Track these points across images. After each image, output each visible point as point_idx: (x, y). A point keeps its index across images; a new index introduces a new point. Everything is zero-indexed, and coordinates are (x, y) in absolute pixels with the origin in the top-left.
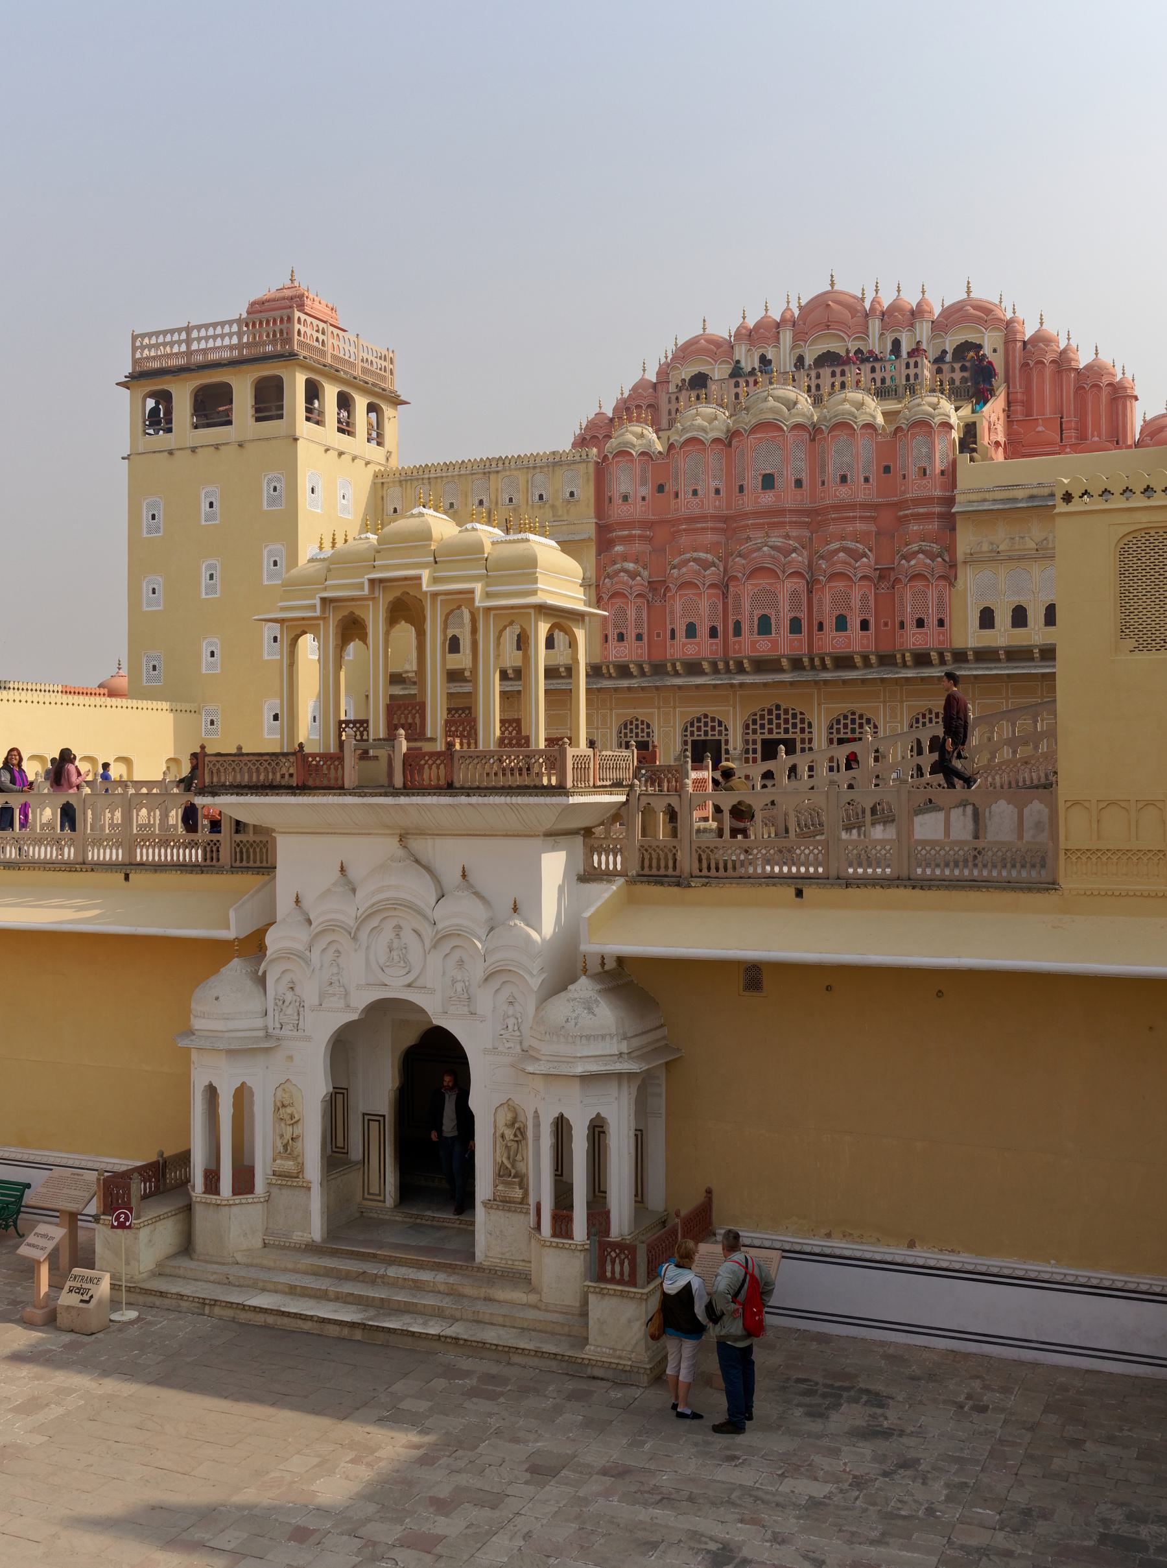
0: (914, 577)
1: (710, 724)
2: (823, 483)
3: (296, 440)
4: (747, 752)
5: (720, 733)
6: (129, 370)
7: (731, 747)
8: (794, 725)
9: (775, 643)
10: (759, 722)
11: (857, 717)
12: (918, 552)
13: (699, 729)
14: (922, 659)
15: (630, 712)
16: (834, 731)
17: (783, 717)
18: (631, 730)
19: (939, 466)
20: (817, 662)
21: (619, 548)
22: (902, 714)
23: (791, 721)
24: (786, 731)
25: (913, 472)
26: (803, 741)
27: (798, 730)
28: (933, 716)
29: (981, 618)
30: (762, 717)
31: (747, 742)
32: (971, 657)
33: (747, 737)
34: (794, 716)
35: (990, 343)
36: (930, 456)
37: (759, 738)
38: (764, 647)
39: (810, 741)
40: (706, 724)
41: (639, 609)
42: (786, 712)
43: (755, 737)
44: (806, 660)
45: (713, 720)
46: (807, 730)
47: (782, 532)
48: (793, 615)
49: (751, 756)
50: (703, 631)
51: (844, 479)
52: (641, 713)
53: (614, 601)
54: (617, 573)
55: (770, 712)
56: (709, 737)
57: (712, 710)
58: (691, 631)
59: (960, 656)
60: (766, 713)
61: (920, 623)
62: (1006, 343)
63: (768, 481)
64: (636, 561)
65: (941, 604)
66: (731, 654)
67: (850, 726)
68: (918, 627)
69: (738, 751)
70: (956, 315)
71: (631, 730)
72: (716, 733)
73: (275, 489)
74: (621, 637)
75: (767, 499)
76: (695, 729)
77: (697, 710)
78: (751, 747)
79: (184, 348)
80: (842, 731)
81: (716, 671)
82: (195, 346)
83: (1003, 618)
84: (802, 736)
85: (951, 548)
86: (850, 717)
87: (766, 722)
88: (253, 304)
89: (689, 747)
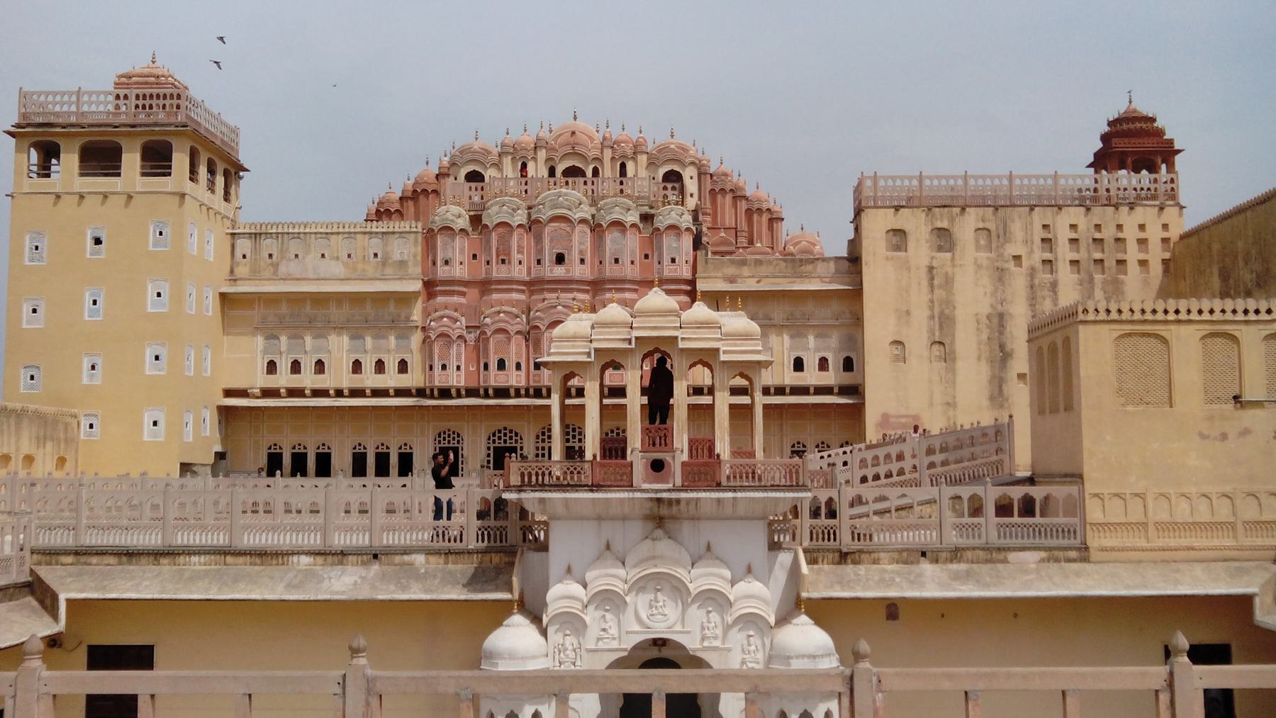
3: (183, 195)
5: (516, 441)
6: (15, 119)
8: (574, 437)
13: (500, 438)
15: (445, 425)
19: (684, 259)
21: (440, 299)
31: (537, 448)
34: (574, 430)
35: (689, 174)
36: (678, 249)
40: (505, 435)
45: (511, 431)
50: (510, 364)
51: (617, 261)
52: (452, 425)
58: (501, 365)
62: (700, 175)
63: (560, 259)
64: (456, 310)
70: (663, 149)
73: (161, 233)
74: (444, 367)
77: (499, 424)
78: (540, 452)
79: (73, 108)
81: (518, 395)
82: (85, 108)
88: (122, 76)
89: (491, 452)
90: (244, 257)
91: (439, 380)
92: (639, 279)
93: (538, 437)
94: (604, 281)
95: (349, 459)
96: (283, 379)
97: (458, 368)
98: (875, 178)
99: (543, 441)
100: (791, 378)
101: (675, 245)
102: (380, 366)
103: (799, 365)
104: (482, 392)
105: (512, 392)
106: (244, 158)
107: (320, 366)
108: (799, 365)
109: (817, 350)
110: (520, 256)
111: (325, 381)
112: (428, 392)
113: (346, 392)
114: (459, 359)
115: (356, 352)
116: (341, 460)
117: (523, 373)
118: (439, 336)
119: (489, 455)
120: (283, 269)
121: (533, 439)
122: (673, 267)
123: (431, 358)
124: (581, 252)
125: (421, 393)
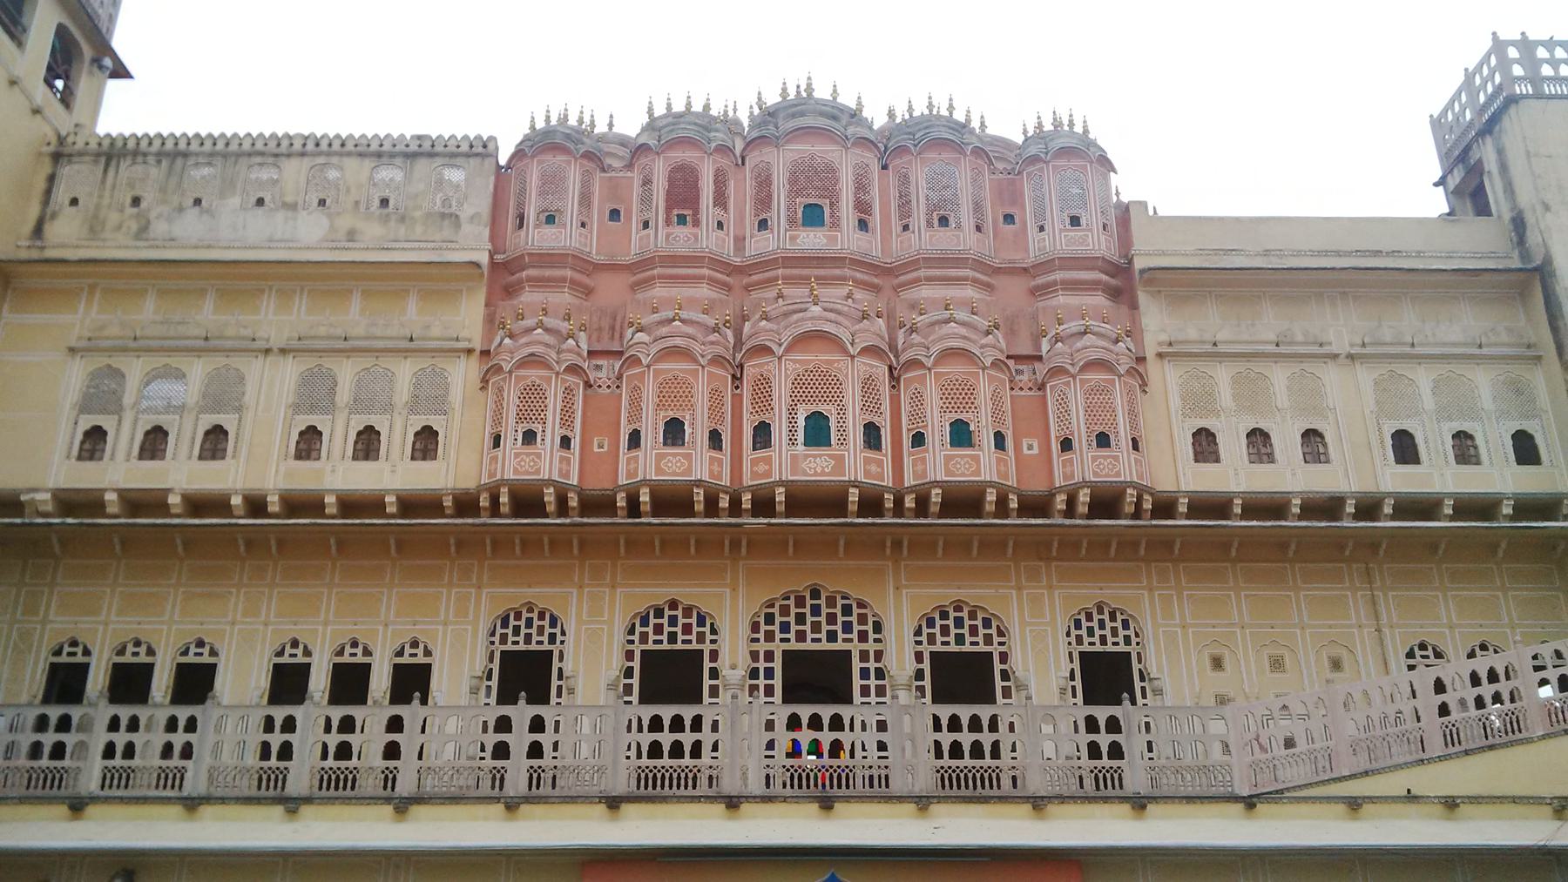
0: (1090, 365)
1: (681, 621)
2: (906, 228)
4: (754, 673)
5: (701, 638)
7: (723, 663)
8: (847, 627)
9: (840, 460)
10: (778, 619)
11: (965, 614)
12: (1085, 333)
13: (658, 629)
14: (1106, 502)
16: (924, 638)
17: (824, 611)
18: (517, 631)
20: (909, 502)
21: (529, 297)
23: (840, 619)
24: (832, 637)
25: (1057, 219)
26: (864, 656)
27: (855, 636)
28: (1106, 617)
30: (785, 611)
31: (754, 656)
32: (1183, 509)
33: (755, 646)
34: (847, 610)
37: (778, 648)
38: (816, 467)
39: (879, 655)
41: (568, 391)
42: (831, 602)
43: (769, 646)
44: (888, 497)
45: (688, 612)
46: (871, 636)
47: (845, 291)
48: (869, 418)
49: (762, 682)
50: (696, 432)
53: (522, 372)
54: (529, 330)
55: (800, 602)
56: (679, 646)
57: (687, 593)
58: (674, 432)
59: (1165, 507)
60: (792, 602)
61: (1103, 440)
64: (567, 317)
65: (1133, 414)
67: (953, 631)
68: (1099, 445)
69: (741, 672)
71: (517, 631)
72: (693, 637)
74: (529, 437)
75: (812, 240)
76: (650, 630)
77: (660, 593)
78: (762, 665)
80: (939, 639)
83: (1232, 445)
84: (864, 646)
86: (952, 615)
87: (792, 619)
89: (636, 664)
90: (74, 202)
91: (514, 465)
92: (996, 263)
93: (755, 627)
94: (913, 264)
95: (261, 681)
96: (119, 472)
97: (566, 442)
98: (1526, 45)
99: (770, 637)
100: (1395, 480)
102: (368, 444)
103: (1405, 448)
104: (621, 502)
105: (699, 496)
106: (123, 42)
107: (215, 442)
108: (1405, 448)
109: (1443, 413)
110: (718, 211)
111: (227, 478)
112: (484, 501)
113: (274, 504)
114: (567, 421)
115: (313, 409)
116: (242, 682)
117: (725, 456)
118: (523, 364)
119: (629, 673)
120: (159, 228)
121: (744, 630)
122: (1075, 234)
123: (497, 421)
124: (862, 207)
125: (466, 504)
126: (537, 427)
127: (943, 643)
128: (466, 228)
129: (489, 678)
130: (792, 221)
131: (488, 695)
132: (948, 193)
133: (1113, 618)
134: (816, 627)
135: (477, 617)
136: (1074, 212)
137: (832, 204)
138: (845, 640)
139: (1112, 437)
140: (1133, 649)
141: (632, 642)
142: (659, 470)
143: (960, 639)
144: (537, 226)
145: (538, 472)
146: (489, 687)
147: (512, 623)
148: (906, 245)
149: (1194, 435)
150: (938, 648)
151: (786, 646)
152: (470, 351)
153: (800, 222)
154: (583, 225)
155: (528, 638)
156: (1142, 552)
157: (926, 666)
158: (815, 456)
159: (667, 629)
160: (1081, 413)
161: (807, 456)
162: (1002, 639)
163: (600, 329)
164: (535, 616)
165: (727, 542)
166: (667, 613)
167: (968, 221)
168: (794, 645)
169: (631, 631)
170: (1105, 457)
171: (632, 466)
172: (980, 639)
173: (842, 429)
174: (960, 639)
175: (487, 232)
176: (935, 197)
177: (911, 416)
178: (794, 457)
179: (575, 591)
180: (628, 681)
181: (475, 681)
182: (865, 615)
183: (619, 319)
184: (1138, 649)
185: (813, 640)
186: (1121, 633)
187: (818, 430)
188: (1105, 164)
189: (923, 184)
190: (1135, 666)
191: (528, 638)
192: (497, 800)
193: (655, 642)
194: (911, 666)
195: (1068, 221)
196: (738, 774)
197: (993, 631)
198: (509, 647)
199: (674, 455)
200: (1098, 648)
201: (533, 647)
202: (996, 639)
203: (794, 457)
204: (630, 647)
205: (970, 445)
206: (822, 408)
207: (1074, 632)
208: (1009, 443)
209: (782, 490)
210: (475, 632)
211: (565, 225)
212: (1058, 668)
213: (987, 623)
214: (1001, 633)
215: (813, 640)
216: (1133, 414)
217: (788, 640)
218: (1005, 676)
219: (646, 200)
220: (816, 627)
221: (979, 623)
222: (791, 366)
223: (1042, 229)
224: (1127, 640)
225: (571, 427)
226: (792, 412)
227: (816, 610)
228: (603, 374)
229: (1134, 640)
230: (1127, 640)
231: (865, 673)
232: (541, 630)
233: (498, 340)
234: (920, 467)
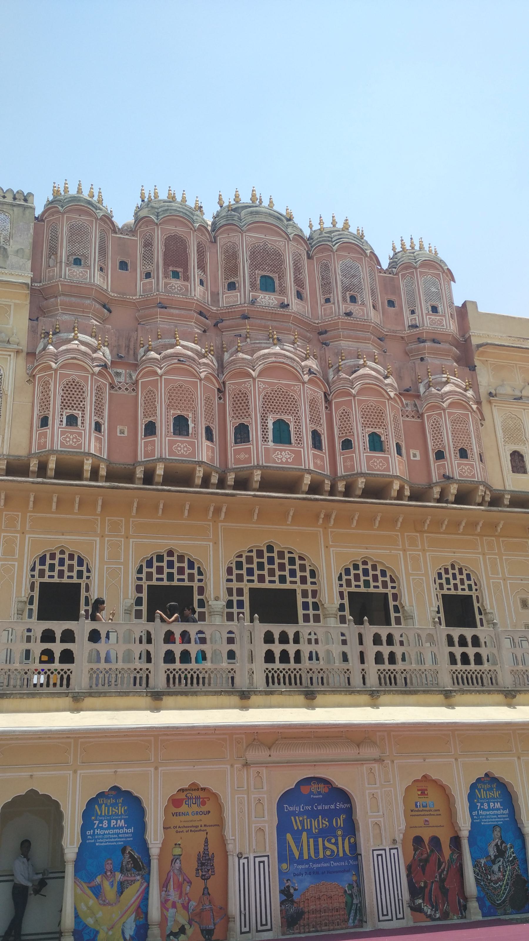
1: (176, 565)
2: (328, 300)
4: (230, 604)
5: (191, 577)
8: (293, 573)
10: (245, 566)
11: (369, 567)
13: (160, 570)
17: (277, 561)
18: (52, 567)
20: (341, 486)
22: (425, 563)
24: (283, 579)
26: (305, 594)
27: (298, 579)
28: (457, 571)
29: (511, 461)
30: (250, 560)
31: (230, 591)
34: (292, 561)
37: (246, 586)
38: (282, 457)
39: (315, 593)
40: (171, 564)
41: (99, 389)
42: (281, 555)
43: (240, 585)
45: (181, 558)
46: (309, 580)
48: (315, 427)
49: (235, 610)
52: (72, 541)
55: (260, 554)
56: (175, 583)
57: (181, 544)
58: (181, 425)
59: (496, 501)
60: (254, 554)
61: (463, 454)
65: (479, 438)
66: (231, 464)
69: (222, 603)
71: (52, 567)
72: (186, 577)
74: (72, 420)
76: (154, 570)
78: (235, 598)
80: (354, 583)
84: (304, 587)
85: (473, 385)
86: (361, 567)
87: (255, 566)
89: (144, 595)
93: (229, 571)
97: (98, 427)
99: (240, 578)
101: (433, 289)
119: (139, 602)
124: (299, 282)
126: (78, 413)
127: (357, 586)
128: (13, 259)
129: (31, 602)
130: (253, 285)
131: (30, 616)
132: (355, 281)
133: (461, 573)
134: (272, 573)
135: (22, 555)
136: (434, 303)
137: (280, 278)
138: (291, 582)
139: (469, 452)
140: (473, 593)
141: (140, 579)
142: (171, 452)
143: (367, 584)
144: (67, 265)
145: (80, 446)
146: (31, 610)
147: (48, 561)
148: (328, 312)
149: (511, 455)
150: (353, 589)
151: (252, 585)
152: (18, 352)
153: (259, 287)
154: (101, 269)
155: (61, 574)
156: (479, 530)
157: (346, 601)
158: (281, 451)
159: (166, 570)
160: (450, 435)
161: (276, 450)
162: (394, 585)
163: (119, 346)
164: (66, 556)
165: (212, 509)
166: (166, 558)
167: (369, 302)
168: (257, 585)
169: (140, 571)
170: (466, 465)
171: (149, 448)
172: (380, 584)
173: (299, 433)
174: (367, 584)
175: (29, 264)
176: (347, 281)
177: (340, 429)
178: (267, 450)
179: (98, 539)
180: (138, 608)
181: (21, 606)
182: (305, 565)
183: (132, 340)
184: (477, 593)
185: (270, 582)
186: (466, 582)
187: (282, 434)
188: (450, 276)
189: (339, 271)
190: (476, 605)
191: (61, 574)
192: (67, 695)
193: (158, 579)
194: (337, 602)
195: (430, 309)
196: (247, 675)
197: (388, 579)
198: (46, 580)
199: (182, 442)
200: (453, 592)
201: (65, 580)
202: (390, 585)
203: (267, 450)
204: (139, 583)
205: (382, 450)
206: (285, 417)
207: (438, 581)
208: (404, 451)
209: (259, 472)
210: (21, 567)
211: (89, 267)
212: (431, 605)
213: (384, 573)
214: (393, 581)
215: (270, 582)
216: (479, 438)
217: (253, 581)
218: (397, 609)
219: (148, 257)
220: (272, 573)
221: (378, 573)
222: (262, 386)
223: (413, 312)
224: (470, 589)
225: (101, 416)
226: (264, 419)
227: (271, 561)
228: (122, 379)
229: (474, 587)
230: (470, 589)
231: (306, 606)
232: (71, 568)
233: (41, 346)
234: (349, 463)
